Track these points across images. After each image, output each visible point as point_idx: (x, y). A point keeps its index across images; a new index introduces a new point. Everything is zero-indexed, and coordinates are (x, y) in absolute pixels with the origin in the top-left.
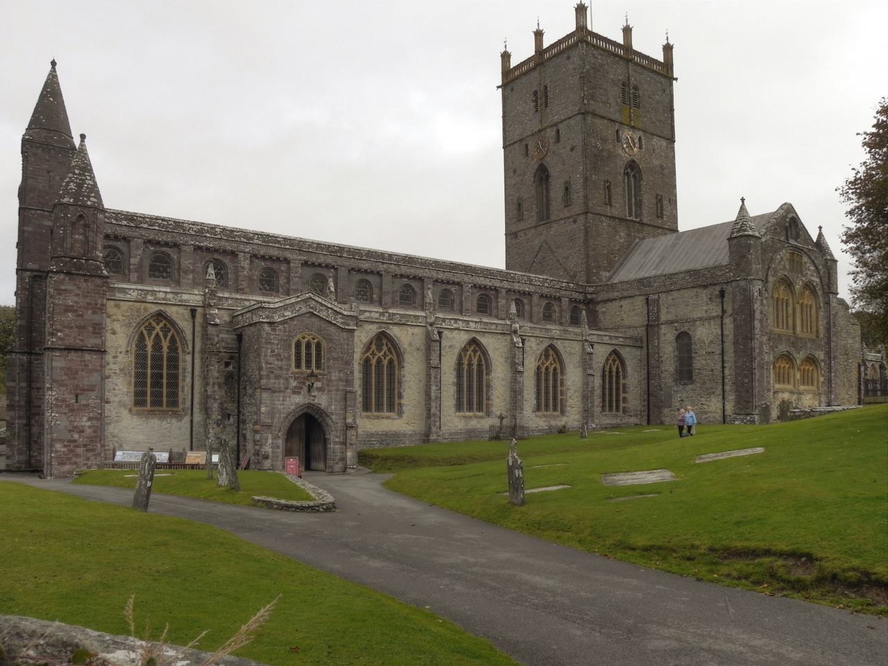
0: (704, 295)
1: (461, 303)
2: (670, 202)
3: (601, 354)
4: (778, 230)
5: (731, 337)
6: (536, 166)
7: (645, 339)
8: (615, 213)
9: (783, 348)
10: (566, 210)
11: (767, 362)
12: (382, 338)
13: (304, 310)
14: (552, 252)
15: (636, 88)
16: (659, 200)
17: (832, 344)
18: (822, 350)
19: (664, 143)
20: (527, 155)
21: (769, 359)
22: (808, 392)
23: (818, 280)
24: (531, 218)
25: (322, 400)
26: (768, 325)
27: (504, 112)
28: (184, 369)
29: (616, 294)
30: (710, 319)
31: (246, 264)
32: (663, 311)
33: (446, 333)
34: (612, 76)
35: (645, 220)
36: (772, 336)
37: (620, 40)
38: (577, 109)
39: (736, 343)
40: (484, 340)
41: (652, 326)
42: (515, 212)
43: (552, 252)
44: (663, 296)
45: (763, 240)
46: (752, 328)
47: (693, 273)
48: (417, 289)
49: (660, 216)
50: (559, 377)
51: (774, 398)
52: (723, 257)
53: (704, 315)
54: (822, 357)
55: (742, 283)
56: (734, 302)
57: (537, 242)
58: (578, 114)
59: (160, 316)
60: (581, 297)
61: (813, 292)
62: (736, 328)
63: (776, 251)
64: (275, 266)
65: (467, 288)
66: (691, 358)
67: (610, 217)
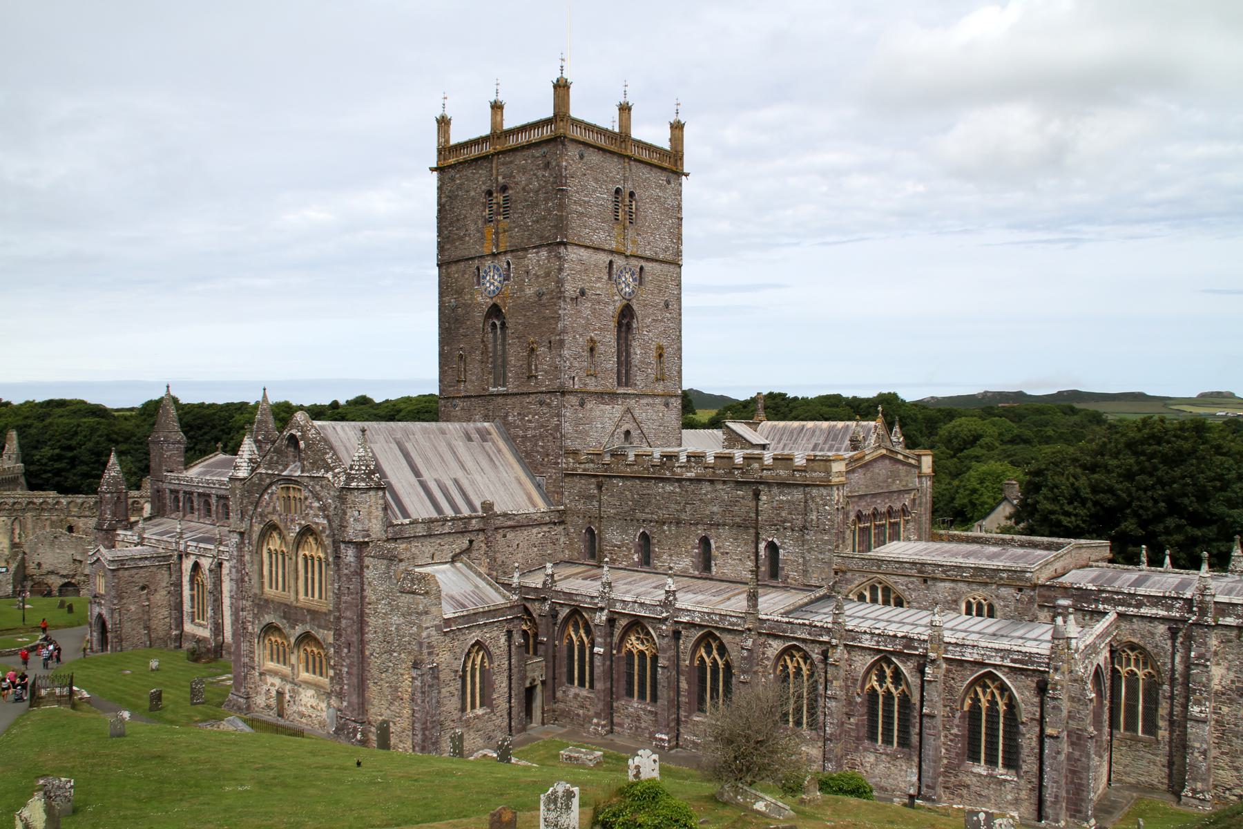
2: (550, 348)
4: (275, 458)
8: (471, 388)
11: (250, 633)
12: (196, 566)
17: (344, 622)
18: (330, 629)
19: (544, 253)
21: (254, 629)
22: (308, 684)
23: (325, 522)
25: (104, 612)
26: (252, 587)
34: (472, 193)
35: (511, 387)
36: (257, 601)
51: (261, 680)
54: (331, 640)
67: (465, 397)
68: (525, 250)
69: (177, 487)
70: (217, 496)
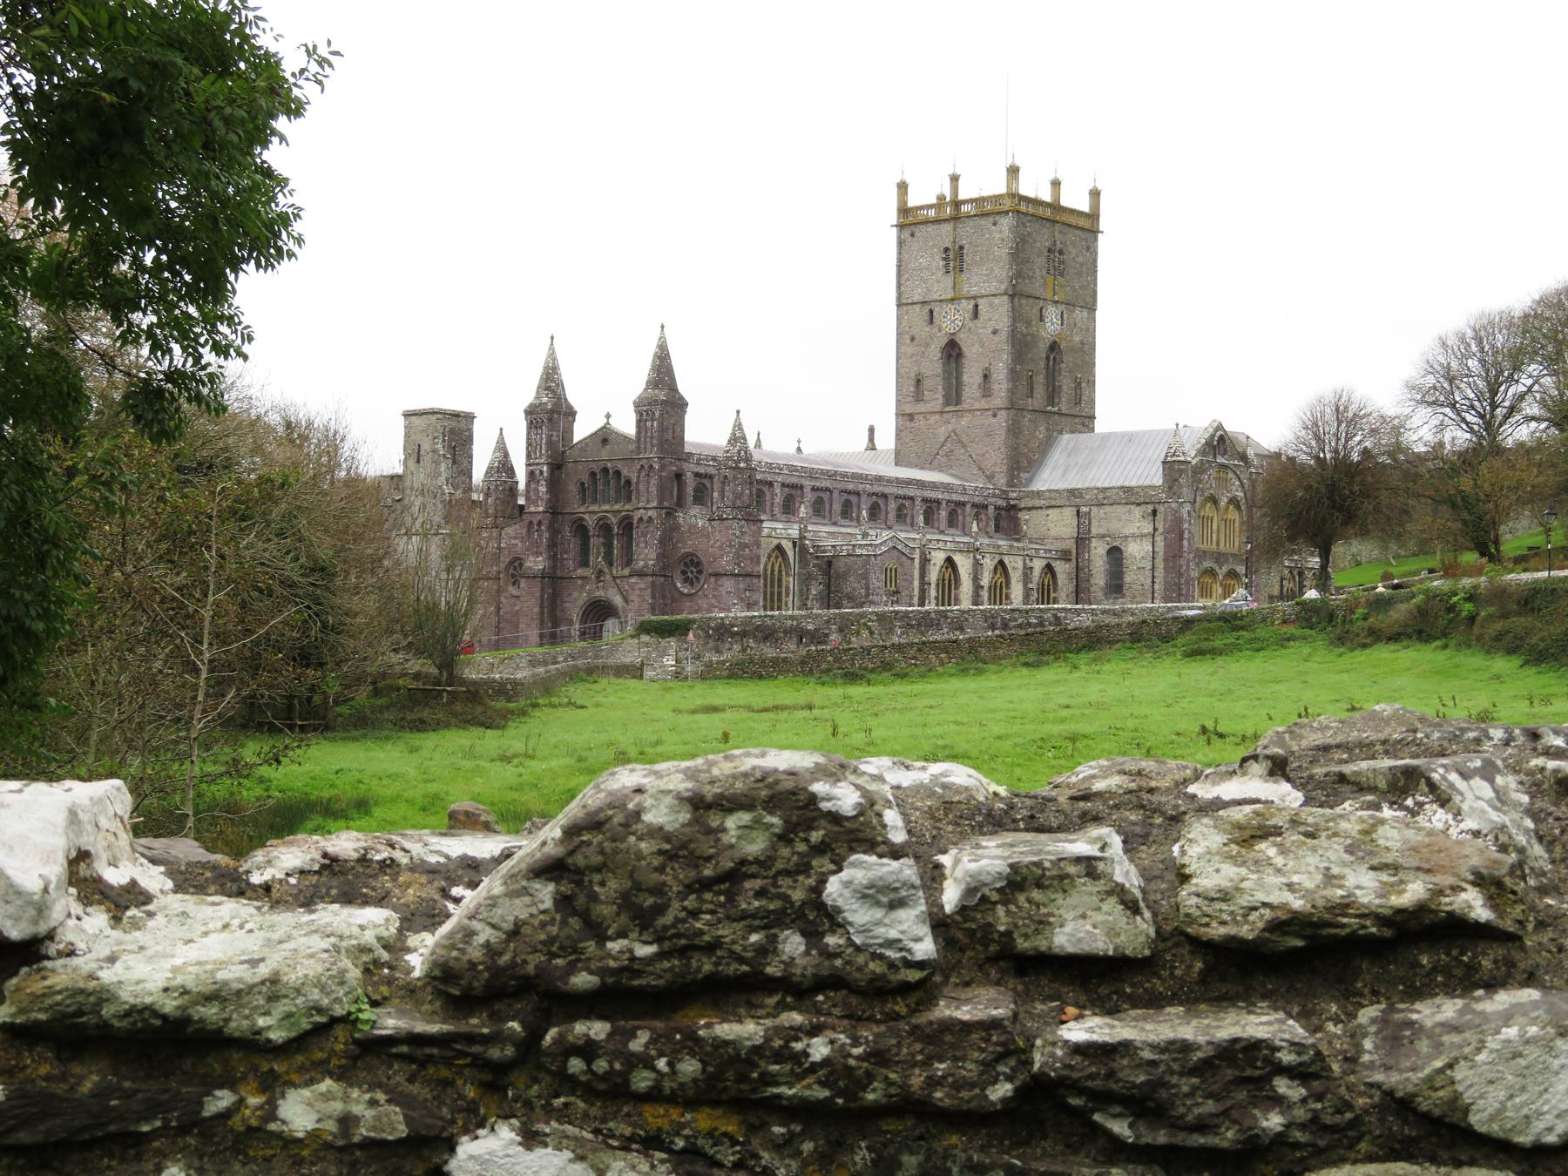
0: (1138, 512)
1: (912, 517)
3: (1038, 565)
5: (1161, 554)
6: (945, 340)
7: (1074, 551)
9: (1207, 564)
10: (983, 400)
13: (891, 545)
14: (964, 446)
15: (1061, 252)
16: (1078, 386)
19: (1085, 314)
20: (931, 322)
24: (935, 399)
27: (900, 260)
28: (787, 588)
29: (1043, 502)
30: (1143, 536)
31: (778, 491)
32: (1094, 523)
33: (933, 553)
35: (1064, 408)
37: (1046, 195)
38: (1003, 287)
39: (1166, 560)
40: (957, 558)
41: (1082, 540)
42: (912, 389)
43: (964, 446)
44: (1094, 509)
45: (1194, 462)
46: (1181, 546)
47: (1127, 490)
48: (882, 506)
49: (1078, 402)
50: (1004, 591)
52: (1157, 479)
53: (1136, 530)
55: (1174, 505)
56: (1165, 521)
57: (942, 431)
58: (1005, 294)
59: (779, 548)
60: (1003, 503)
61: (1238, 507)
62: (1165, 546)
63: (1204, 472)
64: (793, 492)
65: (918, 502)
66: (1122, 573)
68: (1074, 306)
69: (711, 471)
70: (783, 485)
